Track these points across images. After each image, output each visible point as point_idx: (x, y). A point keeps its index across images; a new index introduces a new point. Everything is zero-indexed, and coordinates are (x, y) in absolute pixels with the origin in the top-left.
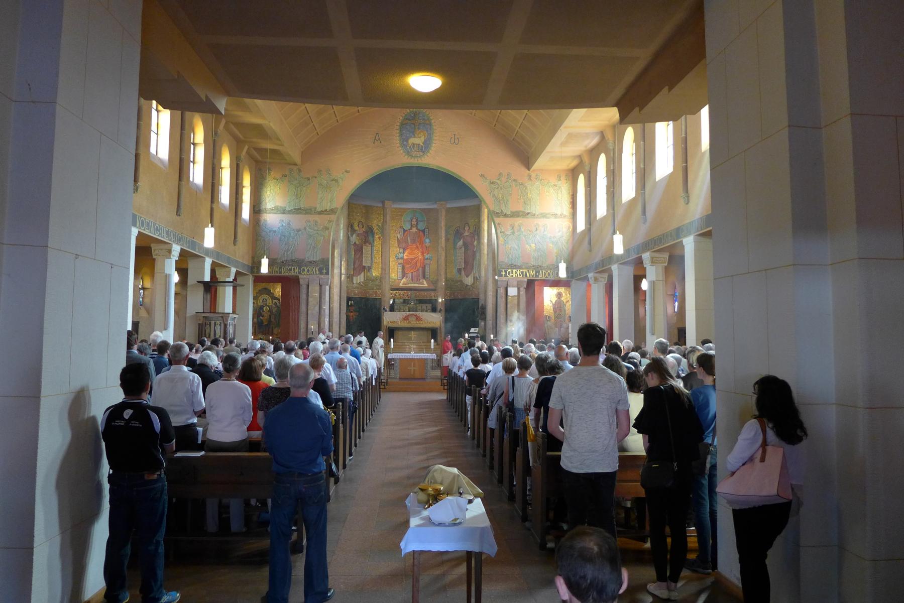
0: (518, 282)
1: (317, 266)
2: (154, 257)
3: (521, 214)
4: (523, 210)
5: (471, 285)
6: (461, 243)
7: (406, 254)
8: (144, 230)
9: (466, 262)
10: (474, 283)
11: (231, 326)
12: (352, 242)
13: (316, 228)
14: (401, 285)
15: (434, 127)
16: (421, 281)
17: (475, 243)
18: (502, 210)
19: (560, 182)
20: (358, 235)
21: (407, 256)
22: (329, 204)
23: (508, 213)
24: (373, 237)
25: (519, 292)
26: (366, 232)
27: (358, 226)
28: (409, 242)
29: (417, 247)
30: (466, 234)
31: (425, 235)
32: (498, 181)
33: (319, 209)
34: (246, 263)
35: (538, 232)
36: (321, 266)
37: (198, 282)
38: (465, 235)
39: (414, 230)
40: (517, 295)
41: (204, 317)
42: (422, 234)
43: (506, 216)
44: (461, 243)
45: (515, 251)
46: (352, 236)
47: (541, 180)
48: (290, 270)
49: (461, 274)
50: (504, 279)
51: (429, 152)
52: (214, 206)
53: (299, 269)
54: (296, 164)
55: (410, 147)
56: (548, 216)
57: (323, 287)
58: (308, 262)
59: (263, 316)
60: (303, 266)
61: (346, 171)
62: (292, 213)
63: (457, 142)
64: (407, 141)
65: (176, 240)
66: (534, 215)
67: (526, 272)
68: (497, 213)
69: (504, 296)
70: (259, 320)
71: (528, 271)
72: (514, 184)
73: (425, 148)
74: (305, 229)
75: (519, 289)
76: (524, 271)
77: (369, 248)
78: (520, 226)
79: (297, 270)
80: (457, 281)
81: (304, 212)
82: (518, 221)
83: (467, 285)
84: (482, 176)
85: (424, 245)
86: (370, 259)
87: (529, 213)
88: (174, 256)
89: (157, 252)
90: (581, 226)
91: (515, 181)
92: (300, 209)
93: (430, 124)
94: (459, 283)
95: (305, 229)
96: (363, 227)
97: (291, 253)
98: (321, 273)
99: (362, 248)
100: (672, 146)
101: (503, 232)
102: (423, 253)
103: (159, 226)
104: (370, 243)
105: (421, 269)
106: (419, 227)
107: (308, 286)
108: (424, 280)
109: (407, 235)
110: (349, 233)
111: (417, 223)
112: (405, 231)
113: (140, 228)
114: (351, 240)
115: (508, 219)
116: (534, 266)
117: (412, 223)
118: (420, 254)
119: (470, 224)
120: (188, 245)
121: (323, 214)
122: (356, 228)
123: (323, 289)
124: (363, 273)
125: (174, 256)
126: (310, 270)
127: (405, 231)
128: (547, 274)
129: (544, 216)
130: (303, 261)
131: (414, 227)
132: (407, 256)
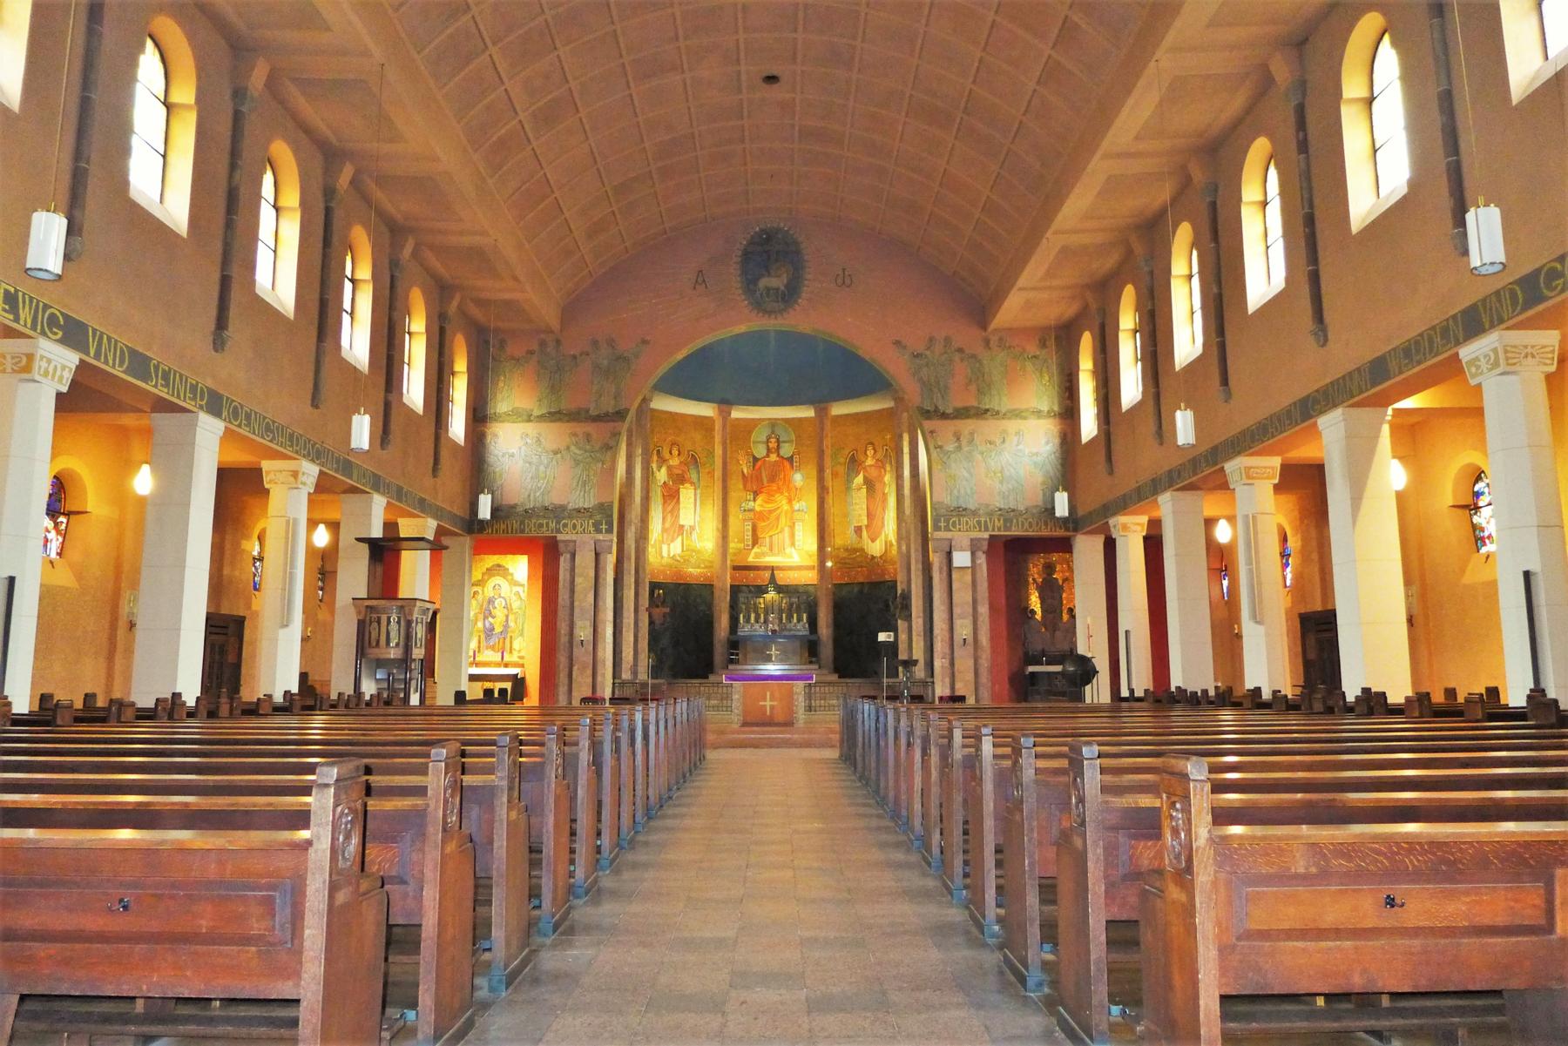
0: (972, 540)
1: (591, 517)
2: (267, 486)
3: (972, 412)
4: (976, 404)
5: (881, 557)
6: (859, 479)
7: (760, 500)
8: (239, 426)
9: (870, 516)
10: (886, 551)
11: (420, 625)
13: (588, 447)
15: (806, 258)
16: (789, 550)
18: (936, 407)
19: (1044, 352)
22: (613, 402)
23: (947, 411)
25: (973, 561)
29: (779, 489)
30: (870, 462)
32: (928, 353)
33: (593, 412)
34: (462, 515)
35: (1006, 445)
36: (598, 517)
37: (359, 540)
39: (773, 457)
40: (969, 565)
41: (367, 607)
42: (787, 464)
43: (944, 416)
44: (859, 479)
45: (964, 483)
47: (1010, 347)
48: (541, 525)
50: (948, 535)
51: (796, 302)
52: (392, 397)
53: (558, 523)
54: (552, 332)
55: (761, 294)
56: (1023, 414)
57: (602, 557)
58: (574, 509)
59: (493, 617)
60: (564, 518)
61: (645, 342)
62: (545, 421)
63: (848, 281)
64: (755, 281)
65: (309, 454)
66: (998, 413)
67: (986, 522)
68: (928, 411)
69: (945, 568)
70: (487, 625)
71: (990, 519)
72: (957, 357)
73: (788, 296)
74: (568, 448)
75: (973, 554)
76: (983, 520)
78: (972, 434)
79: (553, 525)
80: (855, 550)
81: (567, 418)
82: (967, 426)
83: (873, 557)
84: (897, 343)
85: (791, 485)
87: (987, 410)
88: (304, 484)
89: (271, 476)
90: (1089, 426)
91: (960, 350)
92: (559, 412)
93: (798, 252)
95: (568, 448)
97: (543, 494)
98: (598, 531)
100: (1281, 240)
101: (940, 447)
102: (790, 501)
103: (274, 422)
105: (787, 530)
106: (782, 453)
107: (573, 556)
109: (760, 468)
111: (778, 446)
112: (755, 459)
113: (230, 422)
114: (658, 478)
115: (949, 421)
116: (1000, 510)
119: (876, 444)
120: (335, 466)
121: (601, 421)
123: (602, 562)
124: (680, 538)
125: (304, 484)
126: (578, 527)
128: (1026, 525)
129: (1017, 414)
130: (563, 508)
132: (762, 506)
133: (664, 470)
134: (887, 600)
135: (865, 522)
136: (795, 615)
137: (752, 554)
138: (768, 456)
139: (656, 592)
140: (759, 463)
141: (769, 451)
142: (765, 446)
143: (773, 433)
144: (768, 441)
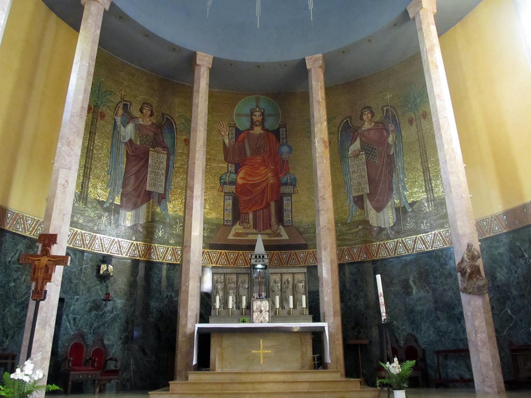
5: (392, 228)
6: (357, 145)
7: (241, 174)
9: (371, 181)
12: (124, 139)
14: (231, 237)
17: (390, 139)
20: (139, 128)
21: (243, 178)
24: (174, 138)
26: (159, 127)
27: (141, 111)
28: (248, 153)
30: (367, 126)
31: (279, 140)
38: (363, 129)
39: (258, 130)
46: (125, 127)
49: (362, 207)
77: (163, 157)
83: (381, 230)
86: (163, 178)
94: (360, 227)
96: (151, 115)
99: (146, 154)
104: (165, 148)
105: (273, 204)
108: (281, 227)
109: (243, 141)
110: (118, 119)
112: (238, 132)
117: (252, 119)
118: (270, 175)
122: (135, 111)
127: (238, 132)
131: (257, 126)
132: (243, 178)
133: (130, 127)
134: (407, 280)
135: (369, 192)
136: (291, 298)
137: (233, 232)
138: (252, 128)
139: (104, 267)
140: (243, 135)
141: (253, 124)
142: (248, 118)
143: (257, 106)
144: (252, 114)
